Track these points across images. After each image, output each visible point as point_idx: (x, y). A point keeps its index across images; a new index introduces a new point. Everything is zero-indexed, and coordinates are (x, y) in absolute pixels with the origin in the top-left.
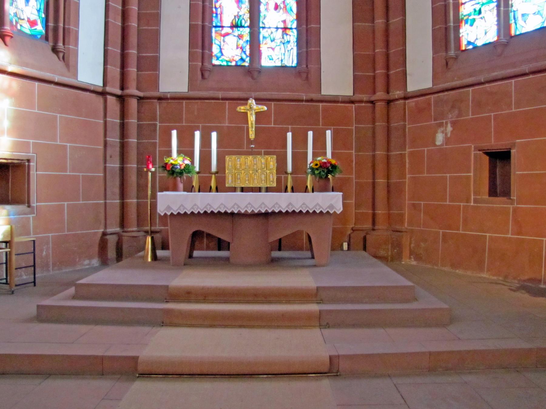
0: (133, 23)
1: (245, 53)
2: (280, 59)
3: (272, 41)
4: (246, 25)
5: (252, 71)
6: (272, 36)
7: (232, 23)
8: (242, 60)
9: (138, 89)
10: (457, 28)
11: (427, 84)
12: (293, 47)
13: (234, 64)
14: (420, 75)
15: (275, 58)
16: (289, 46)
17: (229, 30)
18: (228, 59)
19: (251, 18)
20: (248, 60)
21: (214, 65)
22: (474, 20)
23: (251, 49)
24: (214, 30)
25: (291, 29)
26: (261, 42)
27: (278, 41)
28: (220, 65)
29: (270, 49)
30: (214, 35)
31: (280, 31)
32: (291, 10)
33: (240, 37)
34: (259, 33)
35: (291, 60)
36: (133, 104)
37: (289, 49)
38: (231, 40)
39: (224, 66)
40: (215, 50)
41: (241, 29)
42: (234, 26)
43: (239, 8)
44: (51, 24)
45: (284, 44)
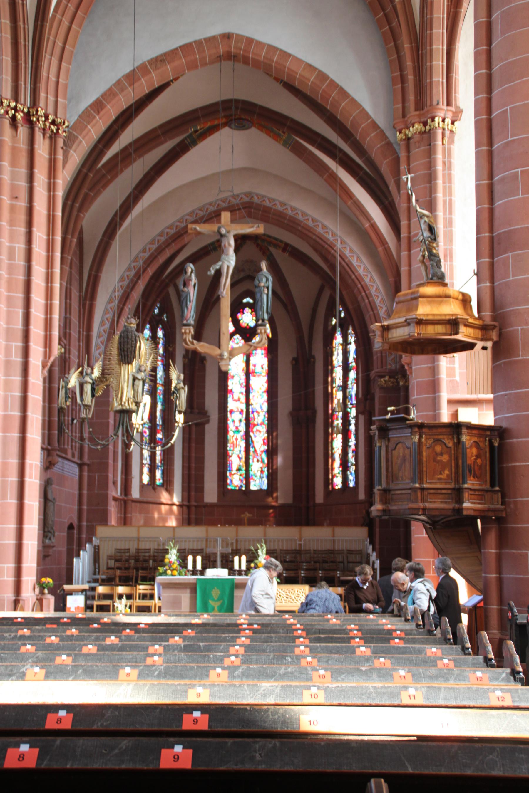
0: (193, 472)
8: (241, 486)
9: (195, 501)
12: (265, 481)
13: (237, 488)
14: (319, 498)
21: (228, 489)
24: (228, 472)
27: (258, 477)
28: (231, 490)
33: (241, 475)
35: (265, 487)
36: (193, 509)
40: (228, 481)
42: (238, 470)
44: (165, 479)
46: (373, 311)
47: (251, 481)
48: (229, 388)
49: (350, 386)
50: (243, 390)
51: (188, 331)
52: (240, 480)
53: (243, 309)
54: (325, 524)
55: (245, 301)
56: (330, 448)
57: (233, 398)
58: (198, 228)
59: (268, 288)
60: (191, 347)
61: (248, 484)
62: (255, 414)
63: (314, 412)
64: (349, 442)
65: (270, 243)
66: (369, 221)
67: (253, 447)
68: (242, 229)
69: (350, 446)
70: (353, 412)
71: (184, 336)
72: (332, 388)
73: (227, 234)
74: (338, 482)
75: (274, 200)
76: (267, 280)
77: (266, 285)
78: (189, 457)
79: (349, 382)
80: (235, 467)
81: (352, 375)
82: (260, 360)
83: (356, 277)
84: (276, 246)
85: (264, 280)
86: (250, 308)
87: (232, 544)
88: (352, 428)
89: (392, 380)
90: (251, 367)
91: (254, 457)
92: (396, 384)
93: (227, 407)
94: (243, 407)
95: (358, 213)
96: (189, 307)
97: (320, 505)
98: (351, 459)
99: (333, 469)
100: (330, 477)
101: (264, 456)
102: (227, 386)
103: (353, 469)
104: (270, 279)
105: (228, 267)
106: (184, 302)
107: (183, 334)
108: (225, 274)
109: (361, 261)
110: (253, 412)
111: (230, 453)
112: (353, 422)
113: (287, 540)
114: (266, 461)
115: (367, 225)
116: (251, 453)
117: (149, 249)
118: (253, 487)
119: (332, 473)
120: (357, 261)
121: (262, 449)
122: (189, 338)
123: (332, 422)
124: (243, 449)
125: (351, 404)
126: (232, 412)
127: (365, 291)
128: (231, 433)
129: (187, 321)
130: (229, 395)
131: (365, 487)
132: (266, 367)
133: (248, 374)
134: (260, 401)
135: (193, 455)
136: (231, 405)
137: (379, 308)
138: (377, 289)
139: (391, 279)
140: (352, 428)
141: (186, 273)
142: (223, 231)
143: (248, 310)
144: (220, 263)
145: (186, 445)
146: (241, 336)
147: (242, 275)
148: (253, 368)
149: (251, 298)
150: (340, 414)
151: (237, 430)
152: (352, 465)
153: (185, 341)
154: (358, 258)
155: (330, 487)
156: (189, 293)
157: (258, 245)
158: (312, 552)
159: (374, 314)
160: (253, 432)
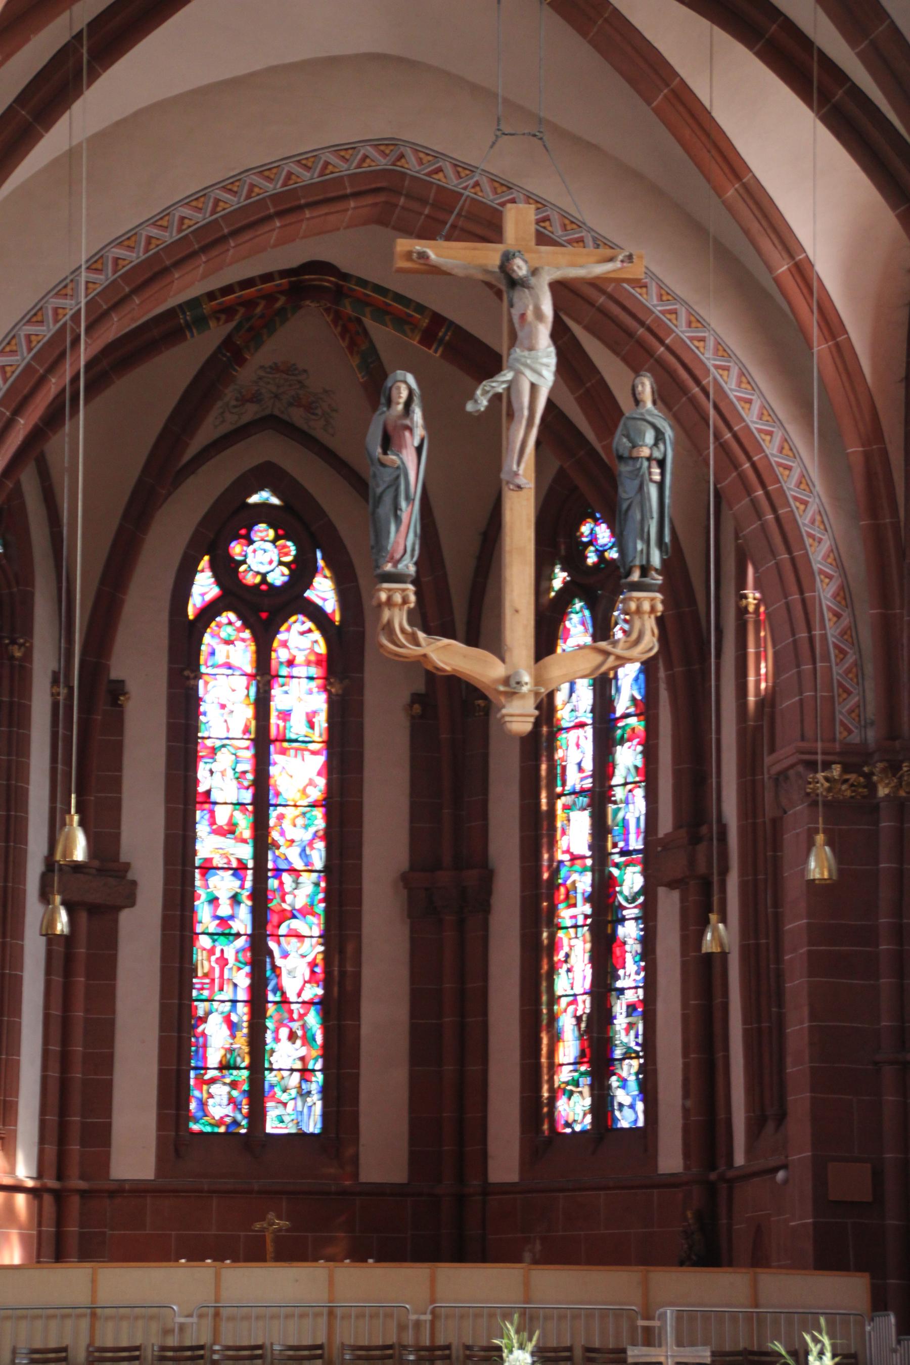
0: (77, 1075)
1: (241, 1112)
2: (295, 1122)
3: (284, 1091)
4: (243, 1065)
5: (250, 1142)
6: (283, 1082)
7: (221, 1062)
8: (236, 1123)
9: (82, 1177)
10: (552, 1100)
11: (513, 1177)
12: (316, 1104)
13: (222, 1130)
14: (504, 1162)
15: (287, 1119)
16: (309, 1099)
17: (215, 1073)
18: (213, 1121)
19: (251, 1053)
20: (244, 1123)
22: (571, 1093)
23: (250, 1104)
24: (192, 1074)
25: (314, 1070)
26: (266, 1094)
27: (294, 1093)
28: (201, 1133)
29: (280, 1105)
30: (192, 1082)
31: (296, 1076)
32: (314, 1040)
33: (234, 1085)
34: (263, 1079)
36: (75, 1202)
37: (310, 1104)
38: (220, 1091)
39: (208, 1133)
40: (193, 1106)
41: (235, 1072)
42: (224, 1066)
43: (233, 1036)
45: (301, 1095)
46: (789, 550)
47: (270, 1105)
48: (201, 789)
49: (619, 793)
50: (247, 796)
51: (398, 598)
52: (231, 1100)
53: (250, 529)
54: (527, 1256)
55: (254, 499)
56: (544, 998)
57: (212, 822)
58: (432, 255)
59: (661, 464)
60: (411, 650)
61: (257, 1114)
62: (286, 877)
63: (487, 877)
64: (618, 978)
65: (381, 313)
66: (792, 257)
67: (279, 988)
68: (573, 265)
69: (621, 991)
70: (632, 880)
71: (386, 614)
72: (553, 797)
73: (533, 281)
74: (574, 1111)
75: (472, 170)
76: (659, 436)
77: (657, 454)
78: (66, 1023)
79: (617, 780)
80: (214, 1058)
81: (628, 757)
82: (303, 702)
83: (735, 436)
84: (402, 323)
85: (649, 437)
86: (271, 525)
87: (418, 1324)
88: (629, 932)
89: (852, 777)
90: (273, 720)
91: (280, 1024)
92: (865, 791)
93: (194, 853)
94: (246, 852)
95: (755, 227)
96: (405, 516)
97: (505, 1189)
98: (625, 1033)
99: (553, 1067)
100: (546, 1094)
101: (313, 1020)
102: (196, 782)
103: (629, 1069)
104: (669, 433)
105: (534, 387)
106: (388, 499)
107: (380, 605)
108: (526, 413)
109: (753, 386)
110: (278, 872)
111: (201, 1008)
112: (631, 912)
113: (604, 1314)
114: (319, 1039)
115: (783, 268)
116: (271, 1009)
117: (56, 310)
118: (276, 1123)
119: (551, 1081)
120: (739, 384)
121: (307, 995)
122: (399, 619)
123: (553, 911)
124: (242, 995)
125: (624, 853)
126: (207, 868)
127: (763, 486)
128: (204, 942)
129: (396, 563)
130: (198, 814)
131: (686, 1130)
132: (321, 721)
133: (264, 741)
134: (300, 834)
135: (79, 1014)
136: (207, 845)
137: (808, 541)
138: (803, 480)
139: (855, 449)
140: (629, 932)
141: (389, 403)
142: (521, 268)
143: (263, 531)
144: (508, 375)
145: (58, 979)
146: (240, 617)
147: (251, 412)
148: (281, 724)
149: (275, 493)
150: (584, 883)
151: (224, 929)
152: (627, 1056)
153: (388, 628)
154: (742, 374)
155: (546, 1127)
156: (402, 470)
157: (338, 317)
158: (578, 1353)
159: (793, 560)
160: (277, 938)
